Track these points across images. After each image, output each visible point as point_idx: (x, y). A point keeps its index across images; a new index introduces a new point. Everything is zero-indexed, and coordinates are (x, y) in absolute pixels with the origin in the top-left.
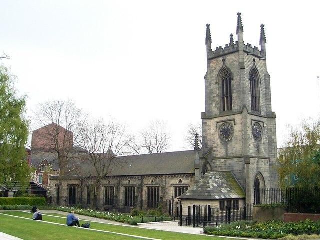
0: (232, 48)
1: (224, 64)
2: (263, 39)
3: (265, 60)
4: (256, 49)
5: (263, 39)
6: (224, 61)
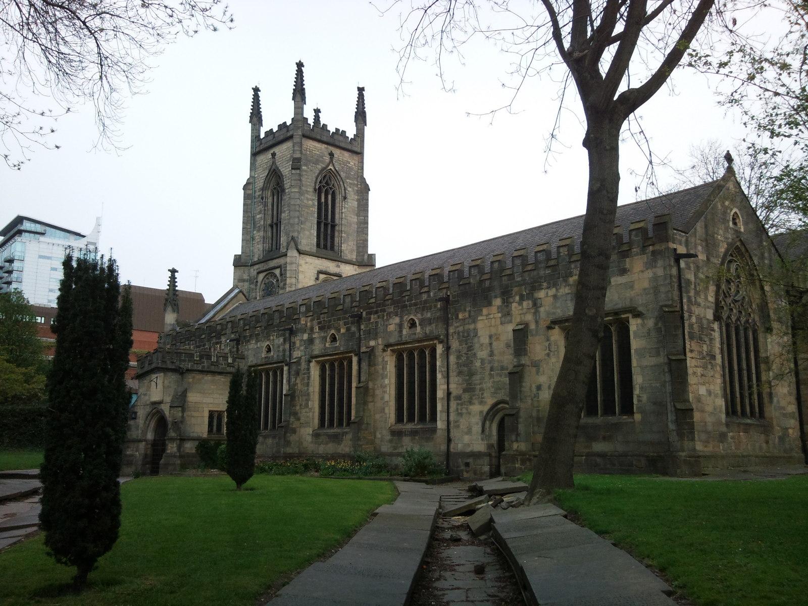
0: (285, 130)
1: (274, 163)
2: (361, 116)
3: (360, 154)
4: (342, 134)
5: (361, 116)
6: (274, 155)
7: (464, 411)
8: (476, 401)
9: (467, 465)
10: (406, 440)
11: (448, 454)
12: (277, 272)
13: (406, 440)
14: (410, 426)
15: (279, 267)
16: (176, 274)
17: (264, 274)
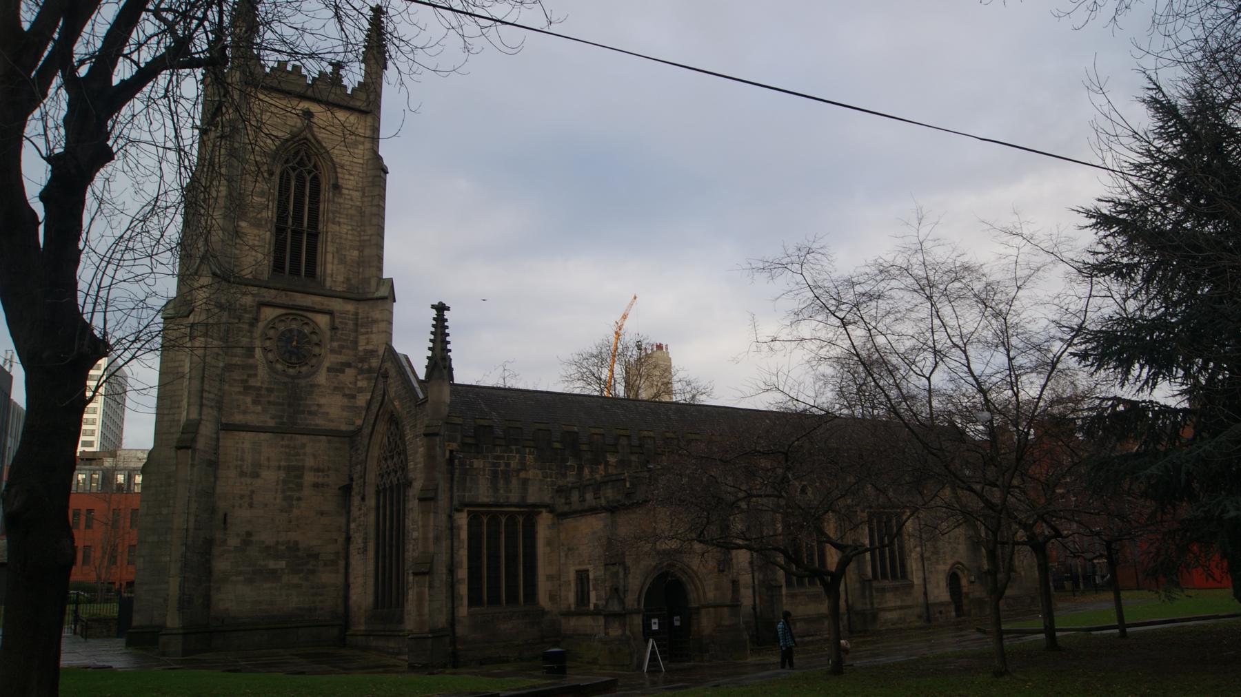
7: (933, 569)
8: (941, 562)
9: (941, 612)
10: (889, 596)
11: (927, 606)
12: (322, 320)
13: (889, 596)
14: (887, 583)
15: (330, 313)
16: (446, 312)
17: (282, 311)
